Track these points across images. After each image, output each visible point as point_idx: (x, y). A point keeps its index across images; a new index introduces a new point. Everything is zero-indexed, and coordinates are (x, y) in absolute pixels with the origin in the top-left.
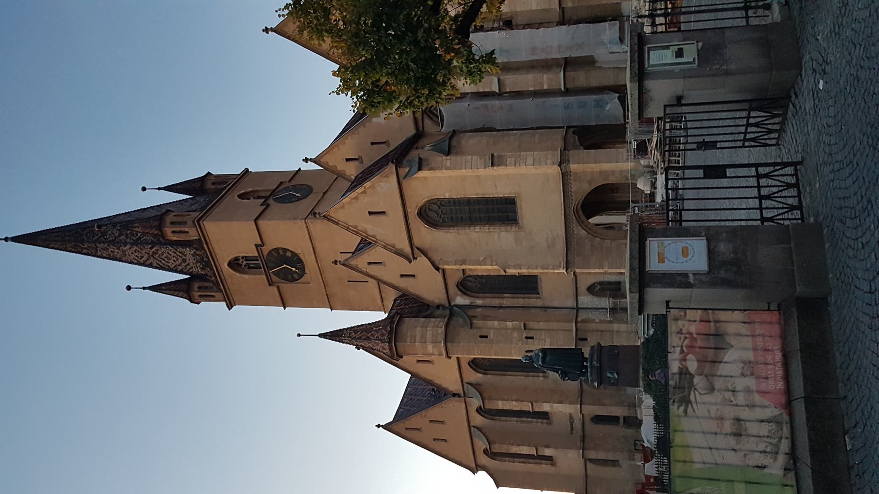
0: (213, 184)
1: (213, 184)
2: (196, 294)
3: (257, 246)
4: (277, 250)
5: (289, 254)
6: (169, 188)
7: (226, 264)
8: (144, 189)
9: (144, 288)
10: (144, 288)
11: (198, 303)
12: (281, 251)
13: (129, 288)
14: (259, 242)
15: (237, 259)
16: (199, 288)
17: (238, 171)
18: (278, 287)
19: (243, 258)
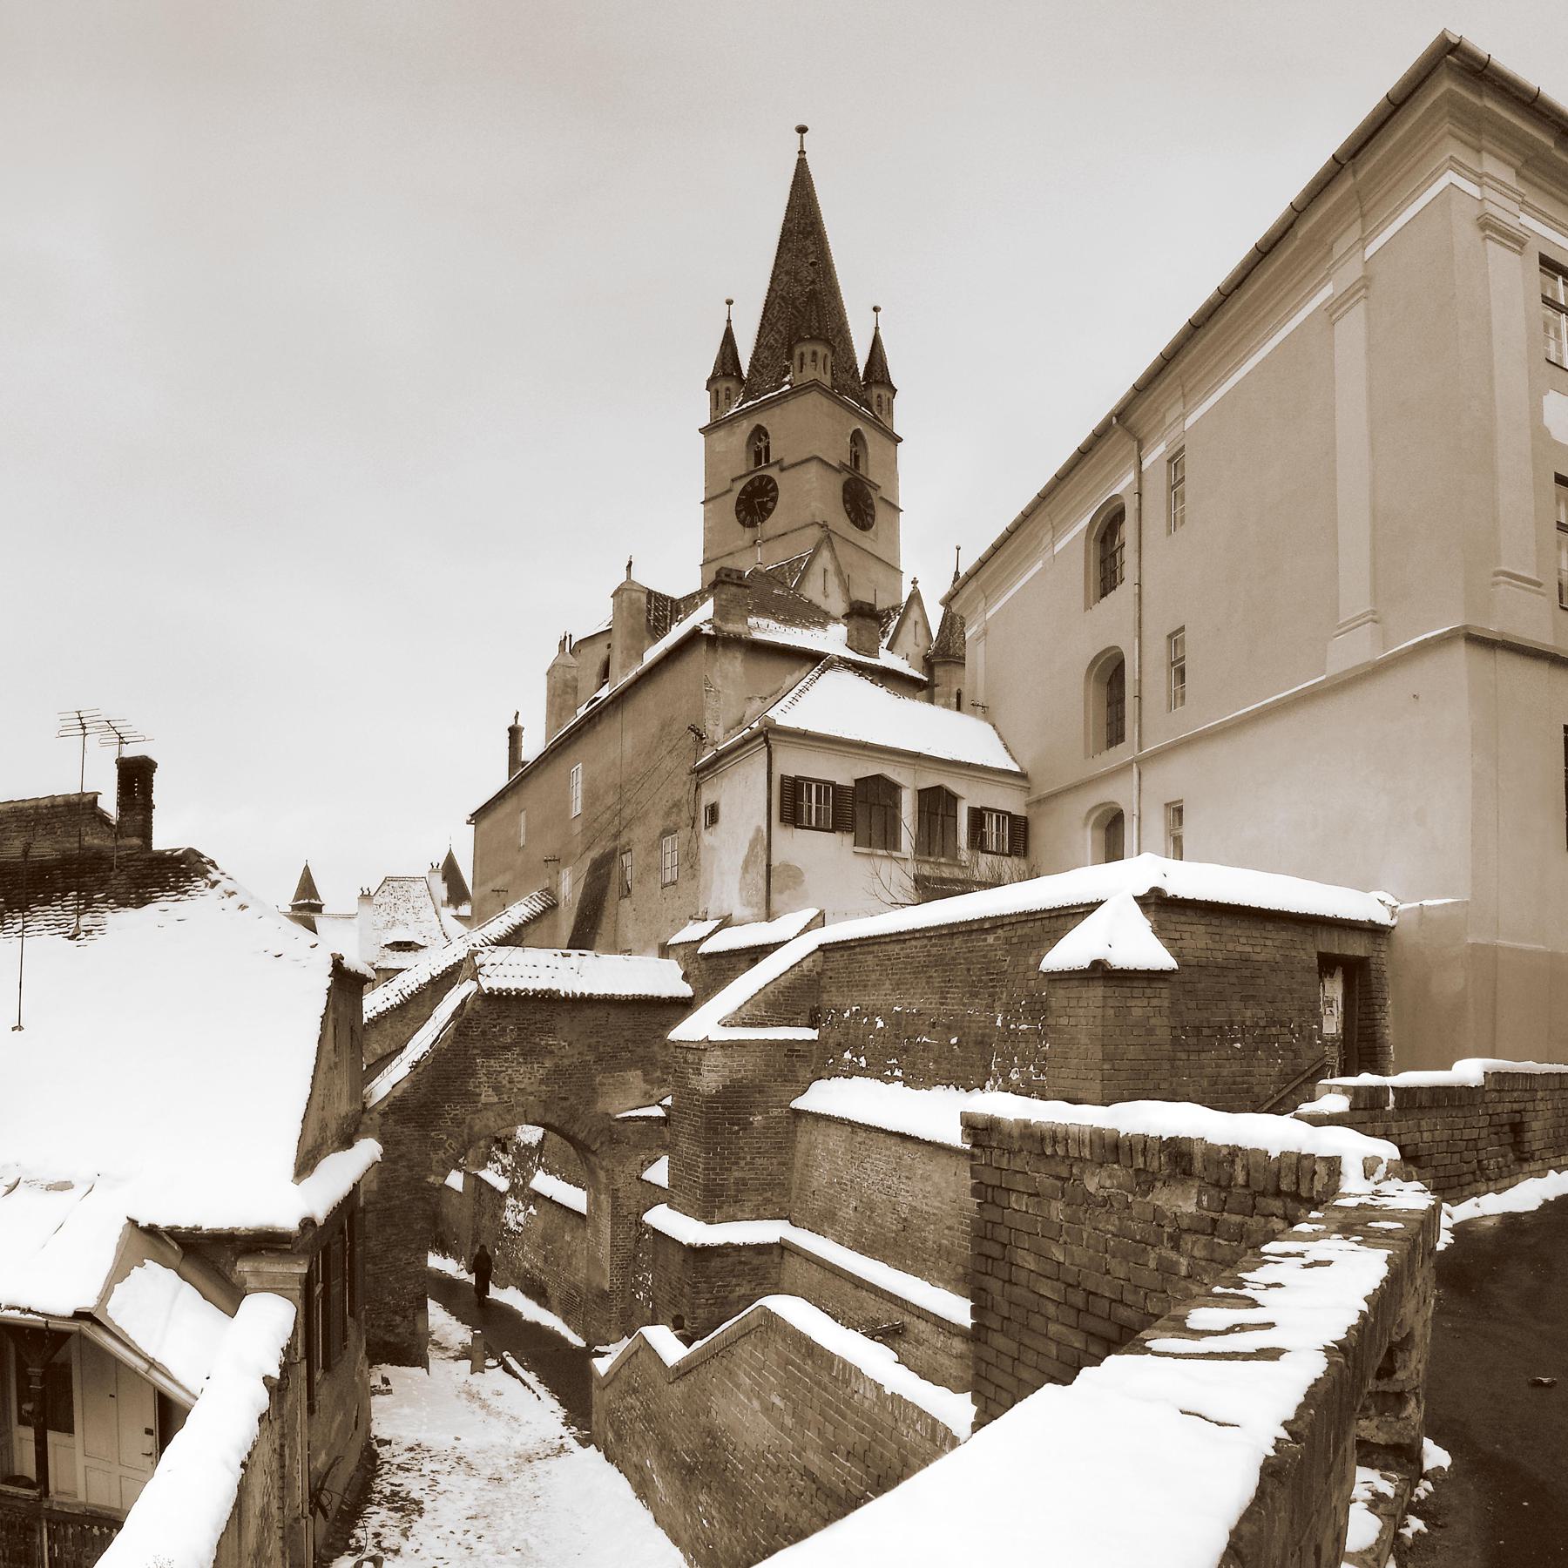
0: (879, 396)
1: (879, 396)
2: (722, 385)
4: (775, 489)
5: (770, 505)
6: (876, 342)
7: (757, 422)
8: (876, 309)
9: (729, 321)
10: (729, 321)
12: (773, 494)
14: (786, 463)
15: (766, 435)
16: (728, 389)
17: (897, 430)
18: (729, 491)
19: (768, 443)
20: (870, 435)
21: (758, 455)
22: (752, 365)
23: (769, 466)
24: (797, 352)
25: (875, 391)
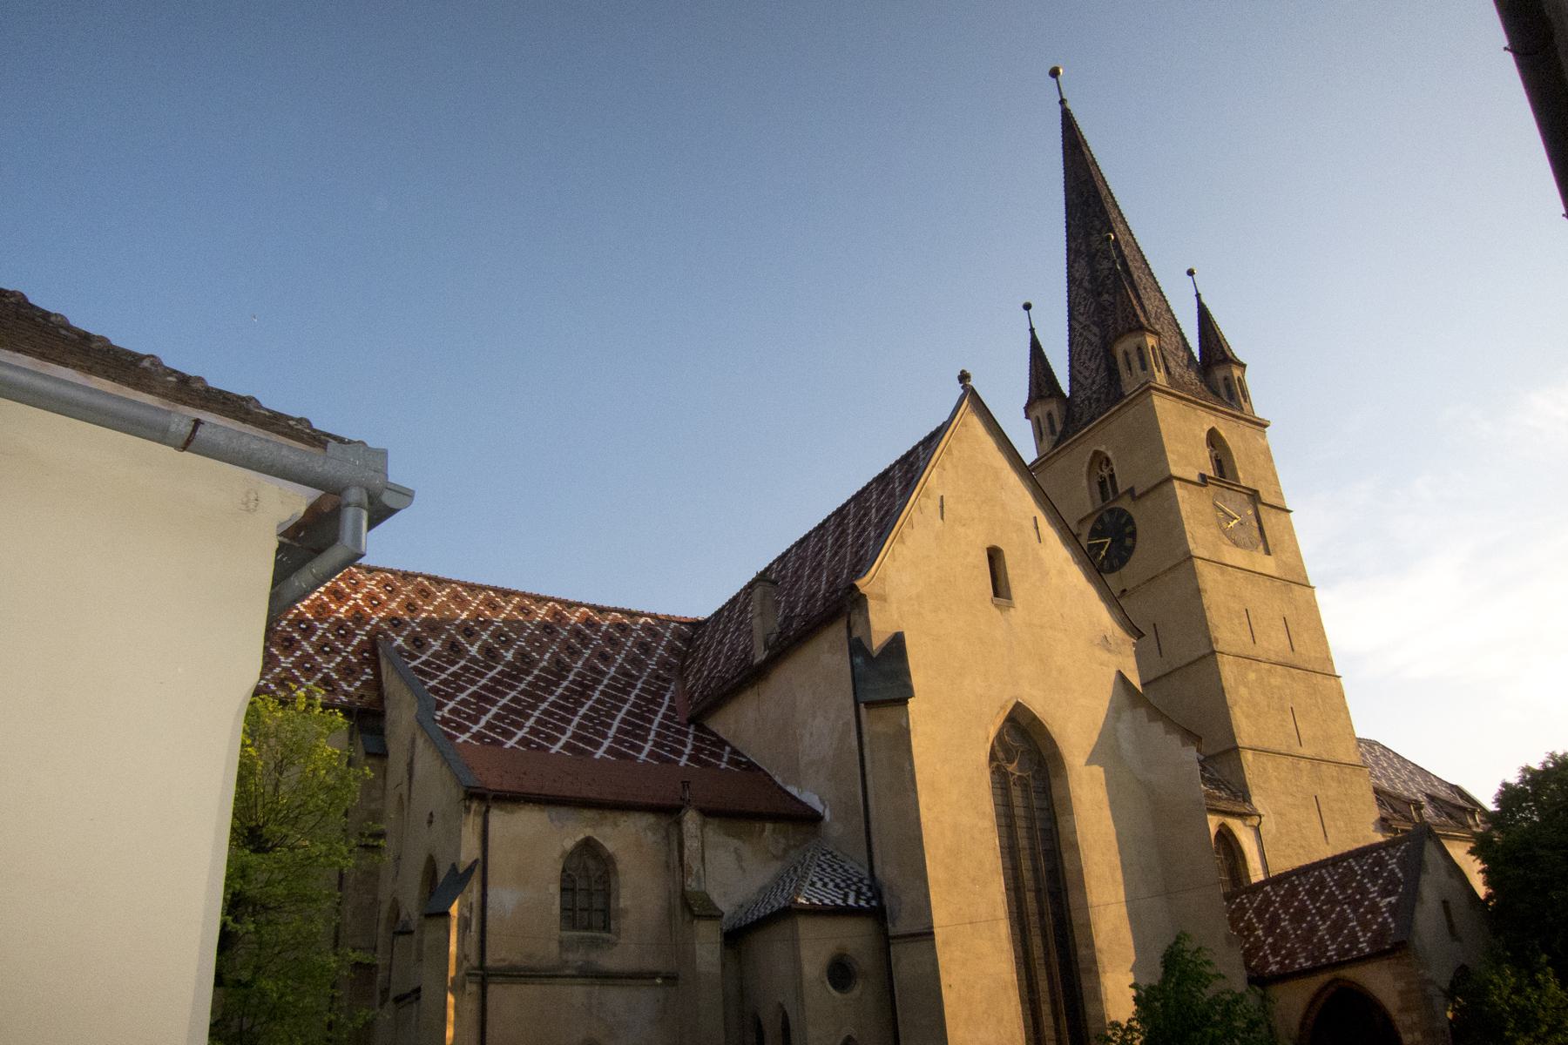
2: (1040, 411)
3: (1131, 491)
4: (1130, 521)
5: (1128, 542)
8: (1191, 273)
9: (1032, 330)
10: (1032, 330)
11: (1027, 417)
12: (1128, 530)
13: (1027, 307)
14: (1138, 492)
17: (1260, 413)
19: (1112, 470)
20: (1226, 429)
21: (1102, 484)
22: (1072, 379)
23: (1118, 497)
24: (1119, 350)
25: (1219, 373)
